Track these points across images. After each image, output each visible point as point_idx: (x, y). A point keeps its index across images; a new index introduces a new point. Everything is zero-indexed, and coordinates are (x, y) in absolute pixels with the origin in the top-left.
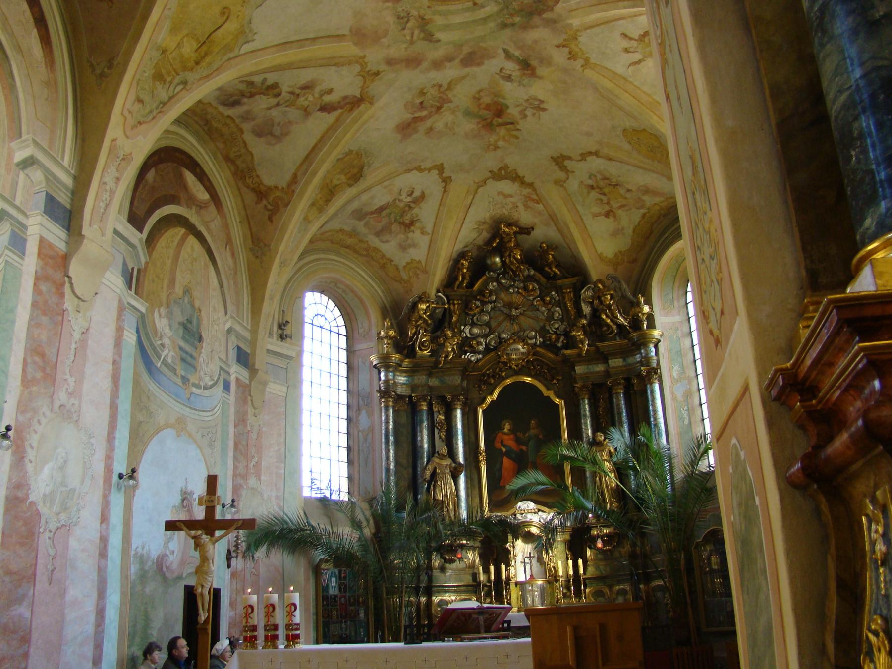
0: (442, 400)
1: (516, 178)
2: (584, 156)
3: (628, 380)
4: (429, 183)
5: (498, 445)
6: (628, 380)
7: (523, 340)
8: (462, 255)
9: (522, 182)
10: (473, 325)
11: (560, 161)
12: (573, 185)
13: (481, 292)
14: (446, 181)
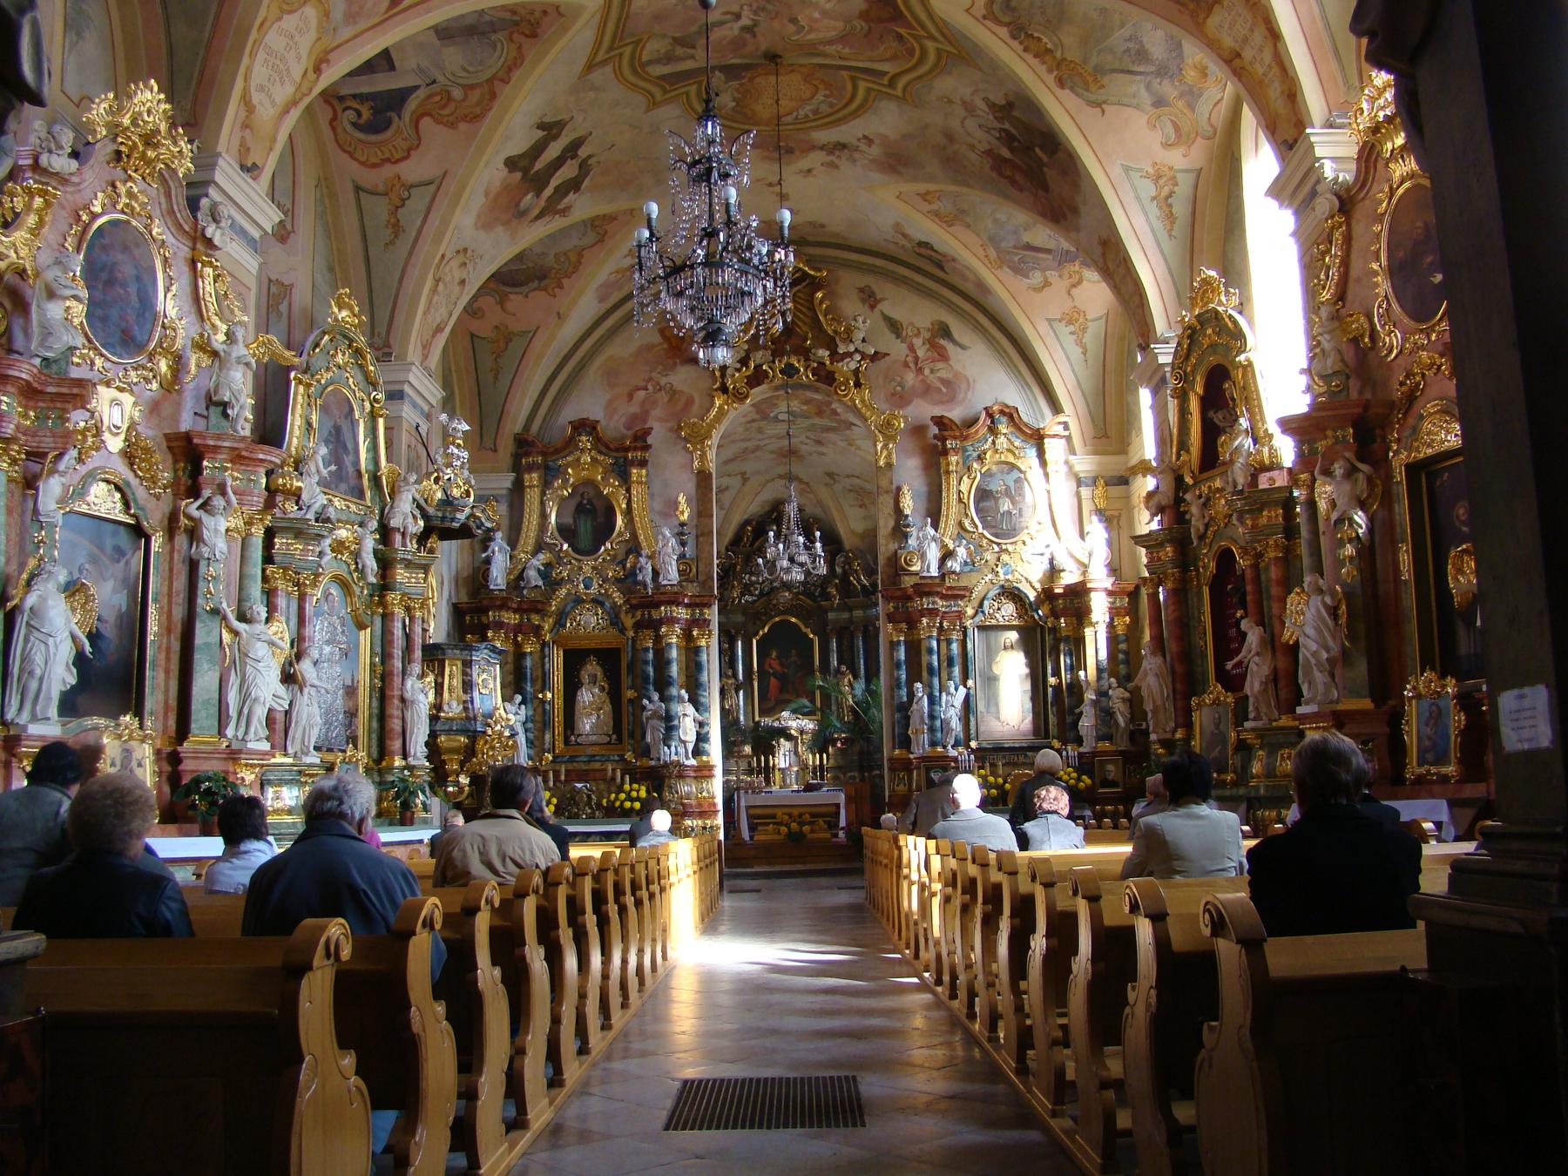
2: (848, 476)
3: (866, 627)
5: (767, 667)
6: (866, 627)
8: (747, 522)
11: (831, 475)
12: (838, 487)
14: (745, 480)
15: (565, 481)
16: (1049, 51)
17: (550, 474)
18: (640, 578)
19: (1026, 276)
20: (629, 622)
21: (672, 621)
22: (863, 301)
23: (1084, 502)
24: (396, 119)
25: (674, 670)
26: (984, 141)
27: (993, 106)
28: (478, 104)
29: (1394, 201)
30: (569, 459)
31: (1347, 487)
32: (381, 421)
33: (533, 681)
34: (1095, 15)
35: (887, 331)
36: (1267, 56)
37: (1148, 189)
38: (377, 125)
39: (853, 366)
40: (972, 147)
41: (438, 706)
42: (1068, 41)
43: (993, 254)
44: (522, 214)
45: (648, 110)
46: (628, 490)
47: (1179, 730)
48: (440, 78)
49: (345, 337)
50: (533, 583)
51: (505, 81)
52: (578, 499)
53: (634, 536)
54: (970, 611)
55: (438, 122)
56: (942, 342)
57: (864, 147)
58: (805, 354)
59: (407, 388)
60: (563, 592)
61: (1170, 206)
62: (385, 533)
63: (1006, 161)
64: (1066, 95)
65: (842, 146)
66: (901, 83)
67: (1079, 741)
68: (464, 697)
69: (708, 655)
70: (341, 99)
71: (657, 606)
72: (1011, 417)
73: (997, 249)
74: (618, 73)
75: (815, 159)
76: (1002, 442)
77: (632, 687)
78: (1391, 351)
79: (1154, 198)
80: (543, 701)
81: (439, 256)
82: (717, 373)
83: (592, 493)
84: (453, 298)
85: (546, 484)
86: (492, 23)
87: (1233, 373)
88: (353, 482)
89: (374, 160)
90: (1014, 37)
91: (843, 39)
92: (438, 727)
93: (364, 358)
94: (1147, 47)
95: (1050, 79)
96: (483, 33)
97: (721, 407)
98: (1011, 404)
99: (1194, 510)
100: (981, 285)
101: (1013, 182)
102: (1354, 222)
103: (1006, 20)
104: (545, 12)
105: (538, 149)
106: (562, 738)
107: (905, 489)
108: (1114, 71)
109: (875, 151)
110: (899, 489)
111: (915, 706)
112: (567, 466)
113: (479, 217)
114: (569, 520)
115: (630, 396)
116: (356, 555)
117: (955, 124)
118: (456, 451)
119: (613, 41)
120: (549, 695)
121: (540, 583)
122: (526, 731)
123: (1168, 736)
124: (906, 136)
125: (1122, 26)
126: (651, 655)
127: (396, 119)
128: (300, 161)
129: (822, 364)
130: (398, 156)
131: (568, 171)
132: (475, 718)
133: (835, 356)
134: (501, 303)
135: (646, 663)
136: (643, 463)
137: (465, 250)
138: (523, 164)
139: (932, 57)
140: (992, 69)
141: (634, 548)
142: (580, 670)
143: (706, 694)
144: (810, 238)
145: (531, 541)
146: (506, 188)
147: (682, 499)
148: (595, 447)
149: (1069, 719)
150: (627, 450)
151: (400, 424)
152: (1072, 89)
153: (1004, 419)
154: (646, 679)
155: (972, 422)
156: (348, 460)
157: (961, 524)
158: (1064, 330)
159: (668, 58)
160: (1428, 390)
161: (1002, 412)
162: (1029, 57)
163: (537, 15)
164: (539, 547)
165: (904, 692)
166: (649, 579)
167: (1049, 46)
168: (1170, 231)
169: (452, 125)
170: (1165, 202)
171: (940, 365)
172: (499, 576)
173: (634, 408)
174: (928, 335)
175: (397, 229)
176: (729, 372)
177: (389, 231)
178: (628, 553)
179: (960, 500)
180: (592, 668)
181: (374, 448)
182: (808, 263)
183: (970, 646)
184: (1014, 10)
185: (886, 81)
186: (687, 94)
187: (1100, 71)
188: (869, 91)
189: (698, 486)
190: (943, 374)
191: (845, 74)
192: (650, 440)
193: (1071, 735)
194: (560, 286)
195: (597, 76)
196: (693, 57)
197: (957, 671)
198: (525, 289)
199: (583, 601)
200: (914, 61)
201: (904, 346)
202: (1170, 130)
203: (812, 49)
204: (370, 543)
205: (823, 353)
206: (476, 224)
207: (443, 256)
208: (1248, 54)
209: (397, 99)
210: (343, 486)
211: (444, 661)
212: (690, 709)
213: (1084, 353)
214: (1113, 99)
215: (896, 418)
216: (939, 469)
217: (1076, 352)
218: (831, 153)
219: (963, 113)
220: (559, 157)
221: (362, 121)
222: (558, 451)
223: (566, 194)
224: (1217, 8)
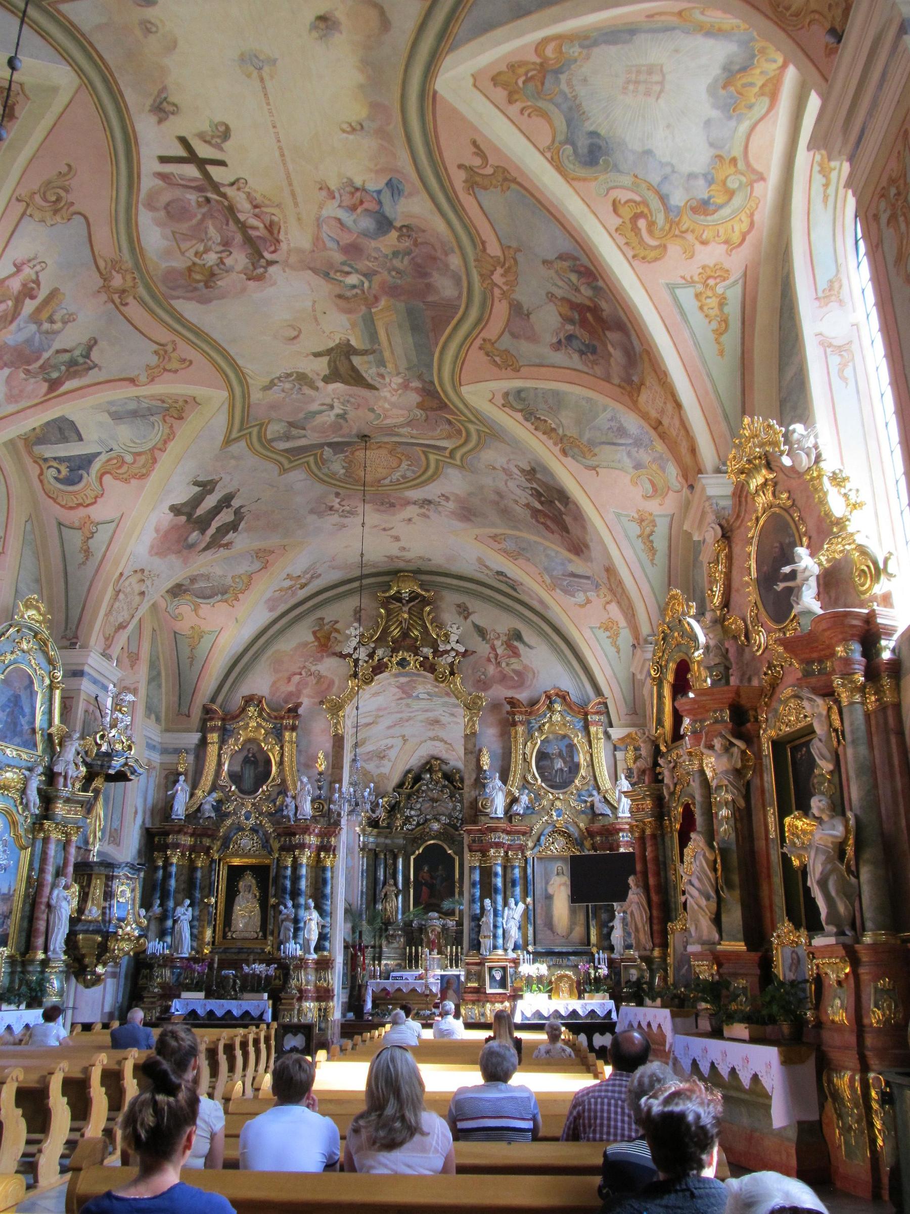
0: (392, 851)
1: (442, 740)
4: (398, 742)
7: (438, 821)
8: (409, 771)
9: (446, 743)
10: (411, 809)
13: (418, 791)
14: (405, 741)
15: (237, 740)
16: (553, 430)
17: (225, 734)
18: (285, 813)
19: (573, 596)
20: (276, 845)
21: (302, 846)
22: (460, 613)
23: (619, 763)
24: (85, 475)
25: (303, 884)
26: (525, 497)
27: (523, 471)
28: (144, 466)
29: (759, 527)
30: (241, 723)
31: (724, 760)
32: (58, 693)
33: (202, 889)
34: (584, 403)
35: (476, 635)
36: (677, 422)
37: (635, 529)
38: (71, 481)
39: (450, 660)
40: (516, 502)
41: (81, 910)
42: (566, 421)
43: (548, 581)
44: (191, 546)
45: (280, 475)
46: (282, 748)
47: (657, 949)
48: (115, 447)
49: (30, 629)
50: (207, 815)
51: (163, 450)
52: (245, 753)
53: (284, 781)
54: (530, 844)
55: (116, 478)
56: (516, 643)
57: (443, 503)
58: (416, 651)
59: (87, 669)
60: (229, 822)
61: (652, 542)
62: (51, 776)
63: (539, 511)
64: (568, 461)
65: (427, 502)
66: (458, 455)
67: (611, 948)
68: (103, 904)
69: (332, 872)
70: (46, 460)
71: (294, 834)
72: (564, 698)
73: (551, 577)
74: (250, 446)
75: (411, 511)
76: (557, 717)
77: (275, 896)
78: (759, 647)
79: (639, 536)
80: (208, 905)
81: (117, 574)
82: (352, 664)
83: (256, 749)
84: (135, 605)
85: (222, 742)
86: (149, 409)
87: (691, 666)
88: (27, 737)
89: (71, 504)
90: (527, 420)
91: (409, 424)
92: (79, 927)
93: (46, 645)
94: (625, 425)
95: (556, 450)
96: (143, 416)
97: (353, 688)
98: (563, 688)
99: (666, 773)
100: (542, 602)
101: (547, 527)
102: (733, 545)
103: (520, 407)
104: (186, 402)
105: (196, 501)
106: (221, 934)
107: (485, 751)
108: (603, 443)
109: (451, 505)
110: (480, 751)
111: (484, 919)
112: (240, 728)
113: (152, 547)
114: (237, 768)
115: (289, 680)
116: (23, 792)
117: (501, 485)
118: (120, 716)
119: (242, 423)
120: (213, 900)
121: (213, 815)
122: (192, 927)
123: (648, 953)
124: (470, 494)
125: (605, 410)
126: (289, 872)
127: (85, 475)
128: (14, 502)
129: (426, 658)
130: (88, 502)
131: (226, 516)
132: (110, 922)
133: (436, 653)
134: (195, 610)
135: (285, 877)
136: (293, 728)
137: (142, 571)
138: (185, 510)
139: (474, 437)
140: (515, 445)
141: (283, 790)
142: (238, 882)
143: (329, 903)
144: (423, 568)
145: (209, 783)
146: (174, 528)
147: (321, 755)
148: (260, 715)
149: (605, 931)
150: (282, 718)
151: (79, 695)
152: (573, 457)
153: (559, 700)
154: (284, 889)
155: (537, 702)
156: (23, 721)
157: (524, 778)
158: (602, 635)
159: (287, 437)
160: (785, 679)
161: (557, 695)
162: (539, 434)
163: (181, 403)
164: (214, 788)
165: (477, 906)
166: (291, 814)
167: (553, 426)
168: (652, 560)
169: (126, 481)
170: (647, 539)
171: (513, 660)
172: (180, 809)
173: (291, 688)
174: (505, 638)
175: (87, 553)
176: (361, 663)
177: (82, 555)
178: (279, 793)
179: (525, 760)
180: (248, 880)
181: (50, 712)
182: (421, 586)
183: (529, 871)
184: (524, 400)
185: (447, 453)
186: (307, 463)
187: (592, 444)
188: (437, 461)
189: (334, 746)
190: (516, 667)
191: (418, 448)
192: (301, 711)
193: (606, 944)
194: (237, 599)
195: (235, 448)
196: (305, 436)
197: (518, 890)
198: (212, 601)
199: (243, 829)
200: (463, 440)
201: (488, 646)
202: (648, 486)
203: (390, 431)
204: (35, 783)
205: (427, 651)
206: (150, 552)
207: (121, 574)
208: (666, 422)
209: (86, 461)
210: (17, 740)
211: (90, 877)
212: (315, 915)
213: (618, 652)
214: (605, 464)
215: (480, 698)
216: (510, 738)
217: (611, 651)
218: (421, 507)
219: (505, 477)
220: (215, 507)
221: (61, 476)
222: (235, 717)
223: (228, 532)
224: (643, 389)
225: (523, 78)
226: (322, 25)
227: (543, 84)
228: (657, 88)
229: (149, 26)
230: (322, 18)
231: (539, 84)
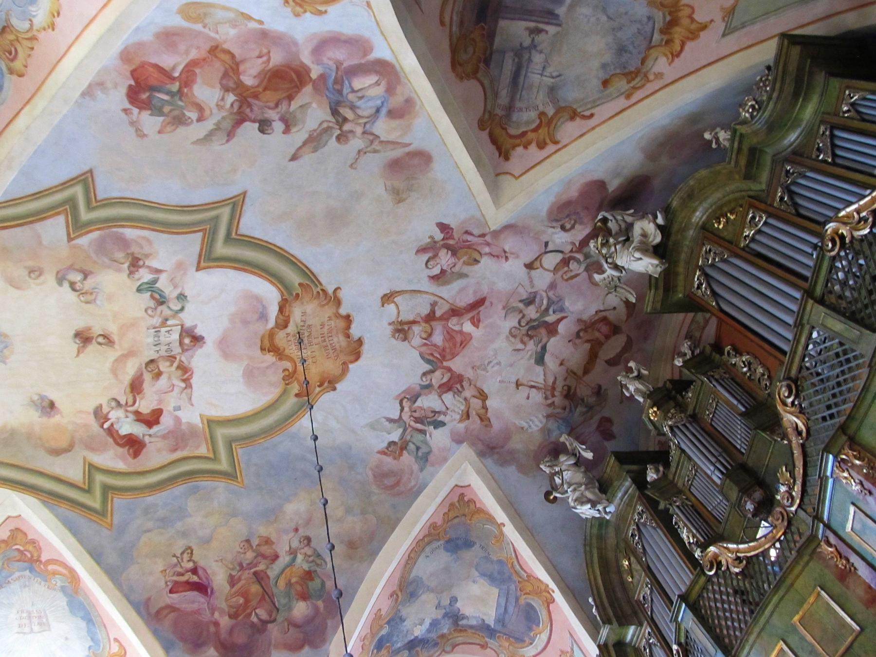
225: (21, 548)
226: (46, 404)
227: (19, 561)
228: (27, 630)
229: (37, 273)
230: (52, 405)
231: (18, 558)
